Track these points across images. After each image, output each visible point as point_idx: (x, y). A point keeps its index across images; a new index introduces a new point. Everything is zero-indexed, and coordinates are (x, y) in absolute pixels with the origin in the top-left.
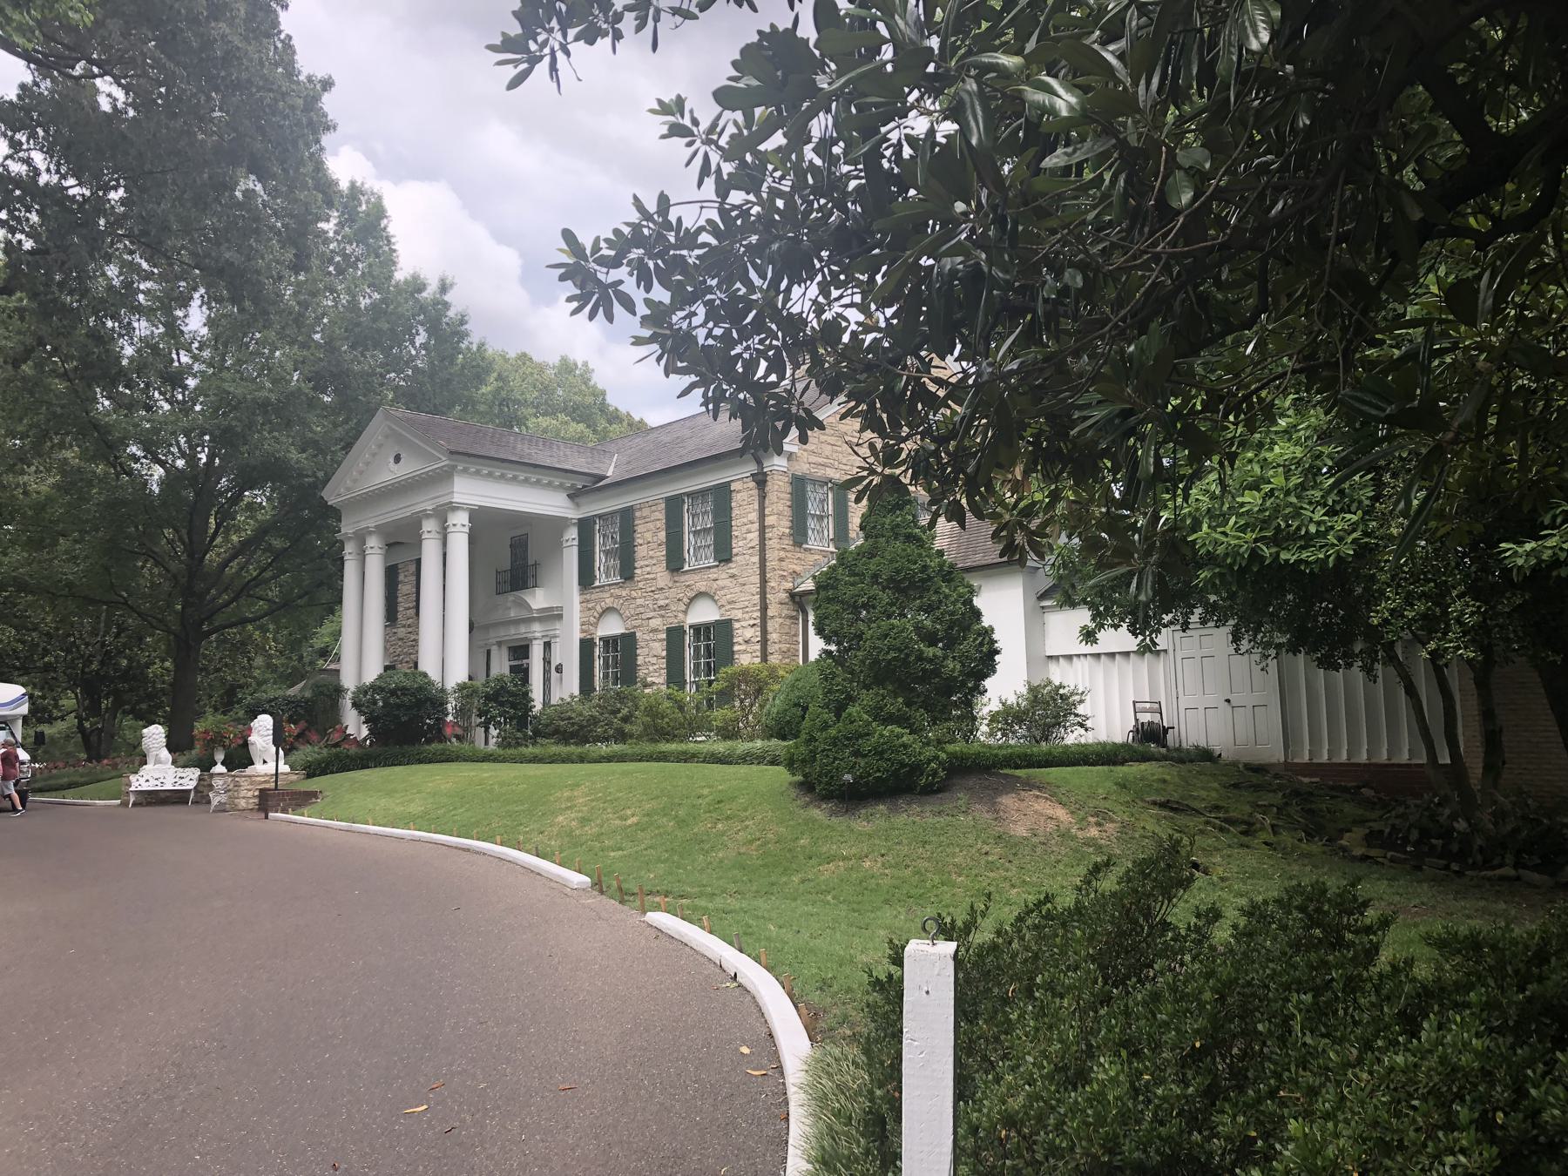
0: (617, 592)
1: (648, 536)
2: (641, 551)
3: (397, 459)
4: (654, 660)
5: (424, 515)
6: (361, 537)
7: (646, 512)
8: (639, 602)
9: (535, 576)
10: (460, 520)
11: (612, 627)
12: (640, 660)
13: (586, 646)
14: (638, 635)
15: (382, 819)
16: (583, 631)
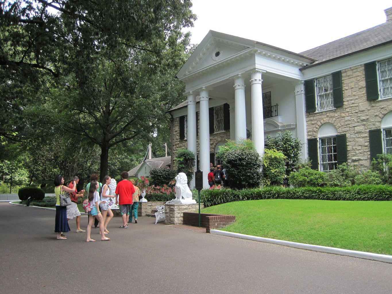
0: (332, 114)
1: (352, 85)
2: (347, 93)
3: (217, 54)
4: (360, 148)
5: (237, 77)
6: (197, 94)
7: (349, 73)
8: (347, 118)
9: (276, 111)
10: (258, 77)
11: (329, 133)
12: (349, 148)
13: (312, 143)
14: (348, 135)
15: (261, 231)
16: (308, 135)
